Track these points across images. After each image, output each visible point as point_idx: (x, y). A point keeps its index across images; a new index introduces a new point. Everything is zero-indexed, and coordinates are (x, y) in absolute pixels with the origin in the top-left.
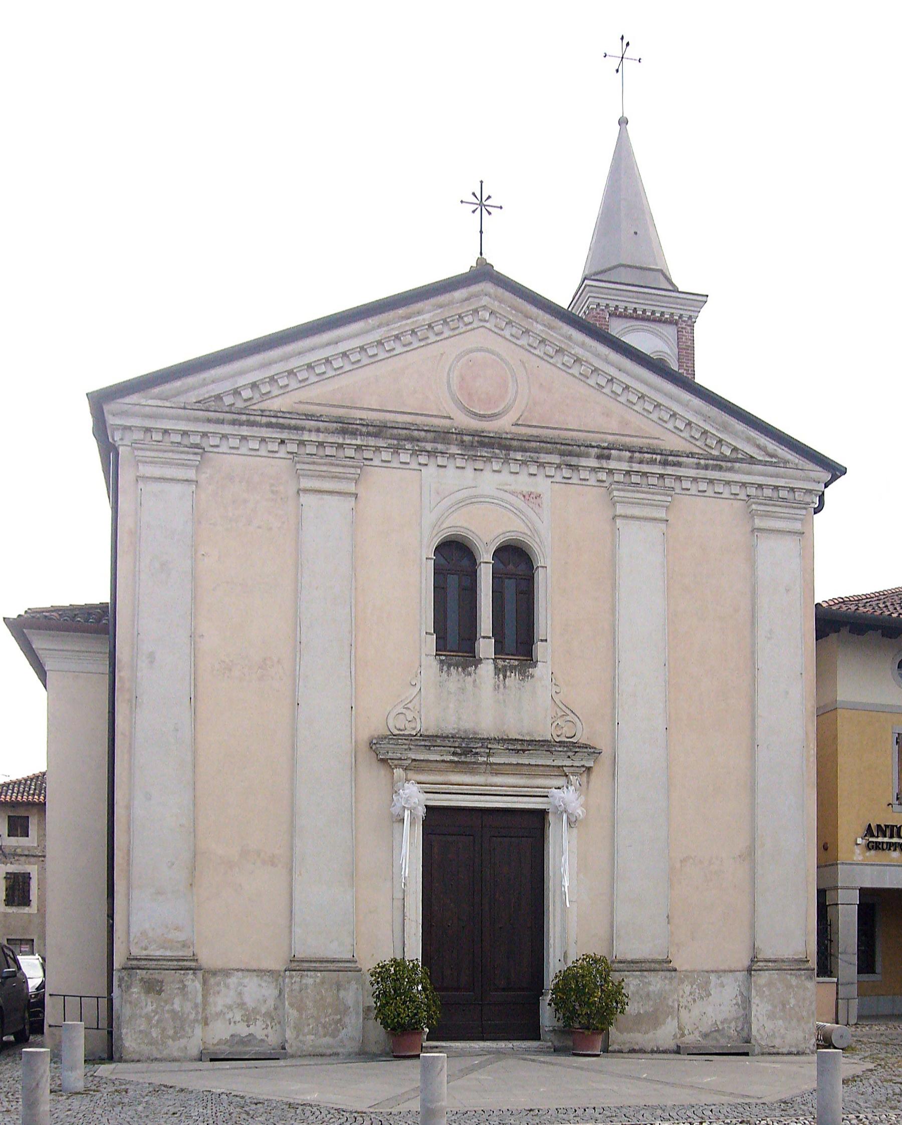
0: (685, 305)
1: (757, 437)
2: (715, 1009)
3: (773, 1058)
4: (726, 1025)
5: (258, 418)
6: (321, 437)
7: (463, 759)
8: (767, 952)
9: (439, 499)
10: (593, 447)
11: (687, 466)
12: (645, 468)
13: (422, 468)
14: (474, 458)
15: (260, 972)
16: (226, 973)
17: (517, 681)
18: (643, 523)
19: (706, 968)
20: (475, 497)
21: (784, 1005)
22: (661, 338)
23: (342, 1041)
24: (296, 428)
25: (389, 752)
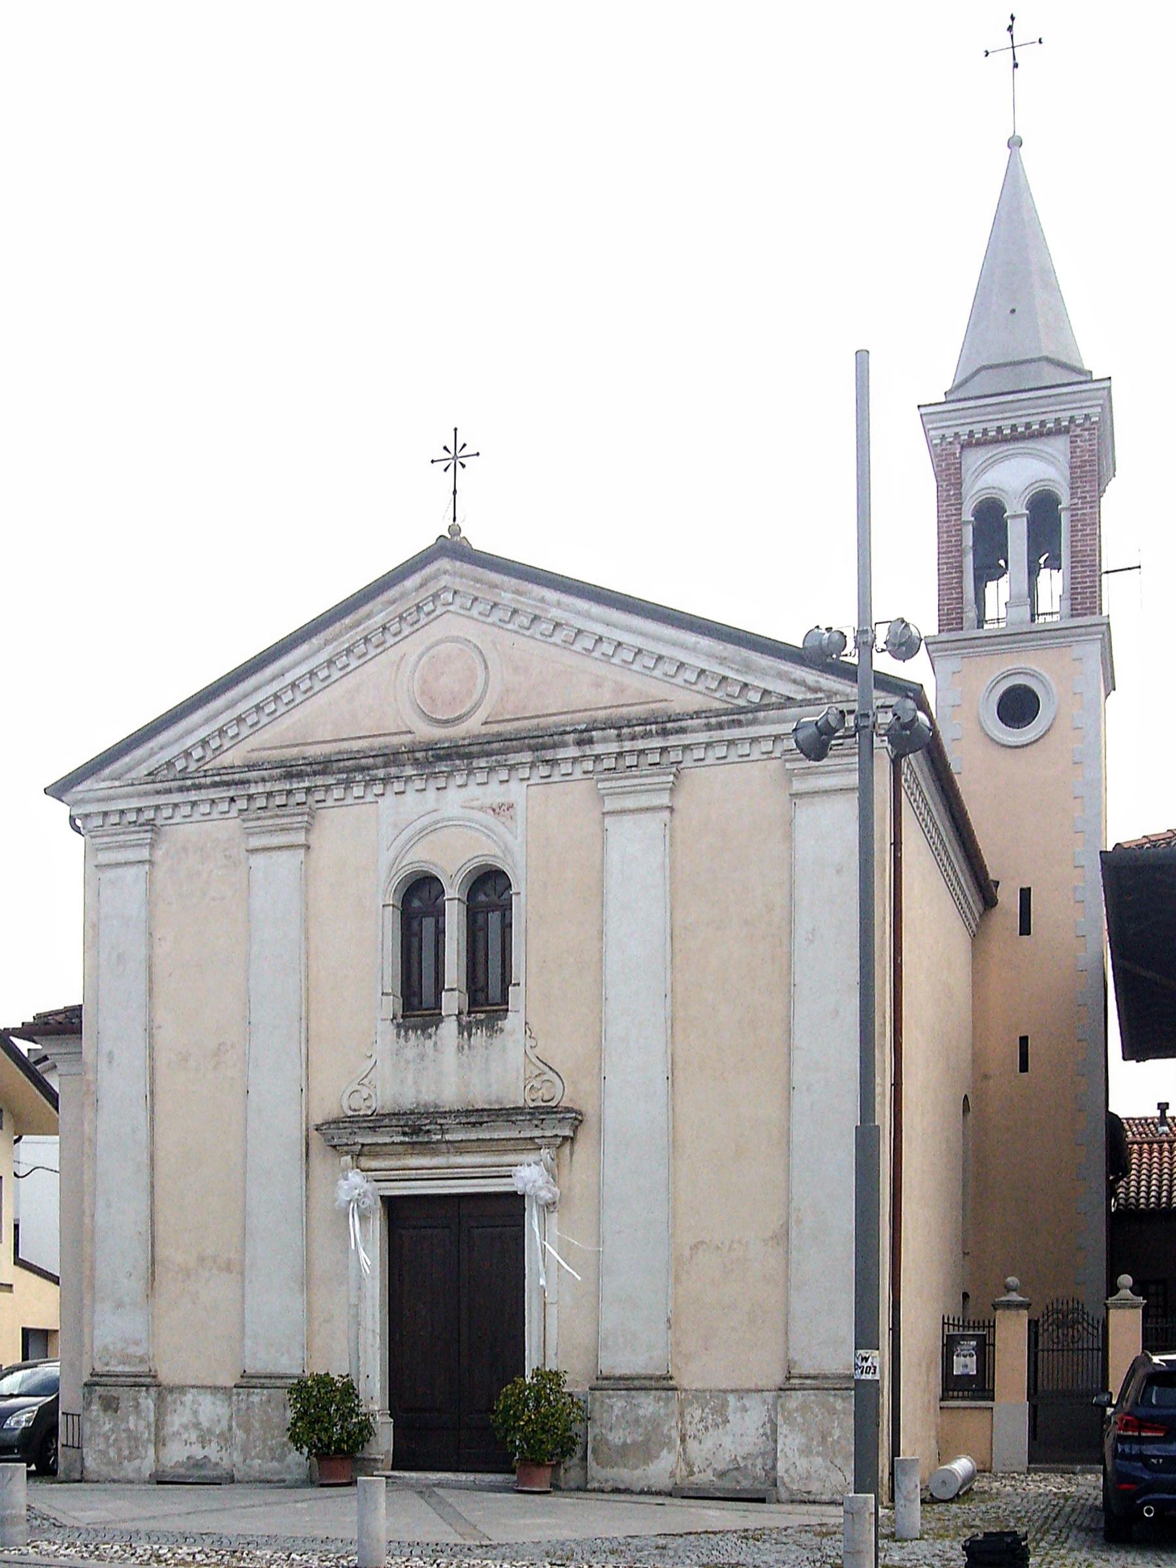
0: (1085, 400)
1: (791, 670)
2: (730, 1441)
3: (805, 1508)
4: (750, 1462)
5: (203, 780)
6: (269, 787)
7: (415, 1139)
8: (806, 1366)
9: (397, 832)
10: (569, 733)
11: (694, 731)
12: (640, 744)
13: (380, 800)
14: (435, 775)
15: (215, 1389)
16: (182, 1389)
17: (485, 1038)
18: (638, 816)
19: (723, 1387)
20: (437, 822)
21: (824, 1438)
22: (1041, 458)
23: (289, 1467)
24: (242, 782)
25: (347, 1135)
